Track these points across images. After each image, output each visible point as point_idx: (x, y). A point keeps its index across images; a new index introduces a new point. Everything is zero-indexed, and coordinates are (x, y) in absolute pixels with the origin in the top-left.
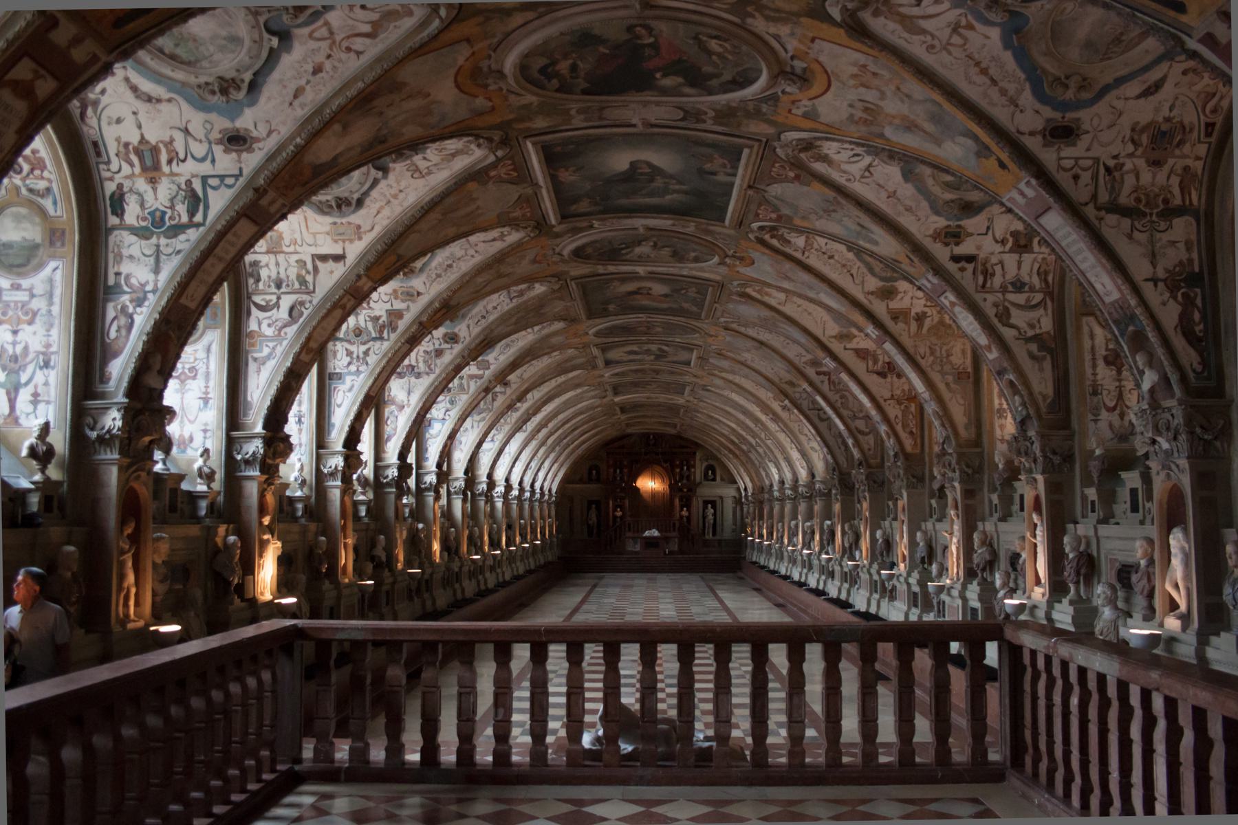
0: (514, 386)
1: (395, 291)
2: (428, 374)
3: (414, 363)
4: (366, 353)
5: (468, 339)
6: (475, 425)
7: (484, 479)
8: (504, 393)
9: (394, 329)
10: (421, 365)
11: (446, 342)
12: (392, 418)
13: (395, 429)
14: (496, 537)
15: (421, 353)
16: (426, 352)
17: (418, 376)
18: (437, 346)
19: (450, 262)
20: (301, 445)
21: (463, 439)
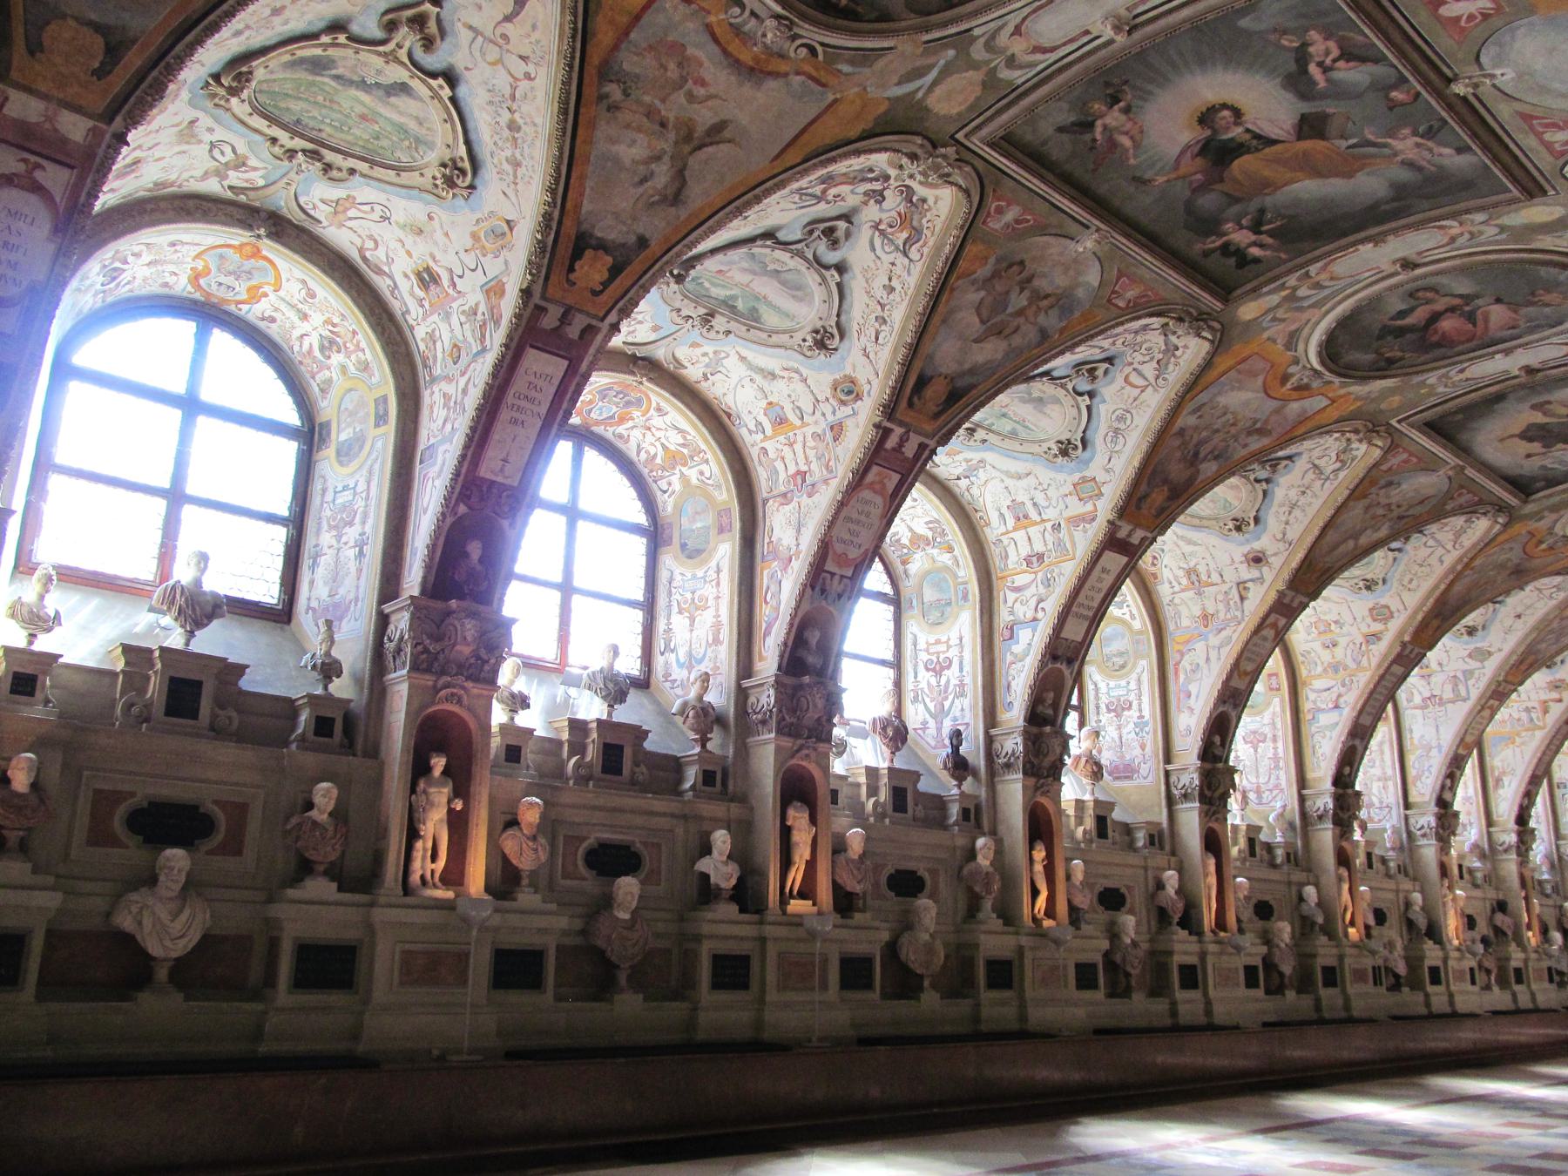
0: (1276, 562)
1: (475, 236)
2: (826, 482)
3: (805, 468)
4: (465, 391)
5: (876, 383)
6: (1213, 655)
7: (1328, 785)
8: (1261, 580)
9: (497, 323)
10: (814, 466)
11: (843, 403)
12: (773, 588)
13: (777, 609)
14: (1422, 922)
15: (811, 443)
16: (816, 436)
17: (812, 490)
18: (830, 418)
19: (506, 116)
20: (357, 599)
21: (1193, 688)
